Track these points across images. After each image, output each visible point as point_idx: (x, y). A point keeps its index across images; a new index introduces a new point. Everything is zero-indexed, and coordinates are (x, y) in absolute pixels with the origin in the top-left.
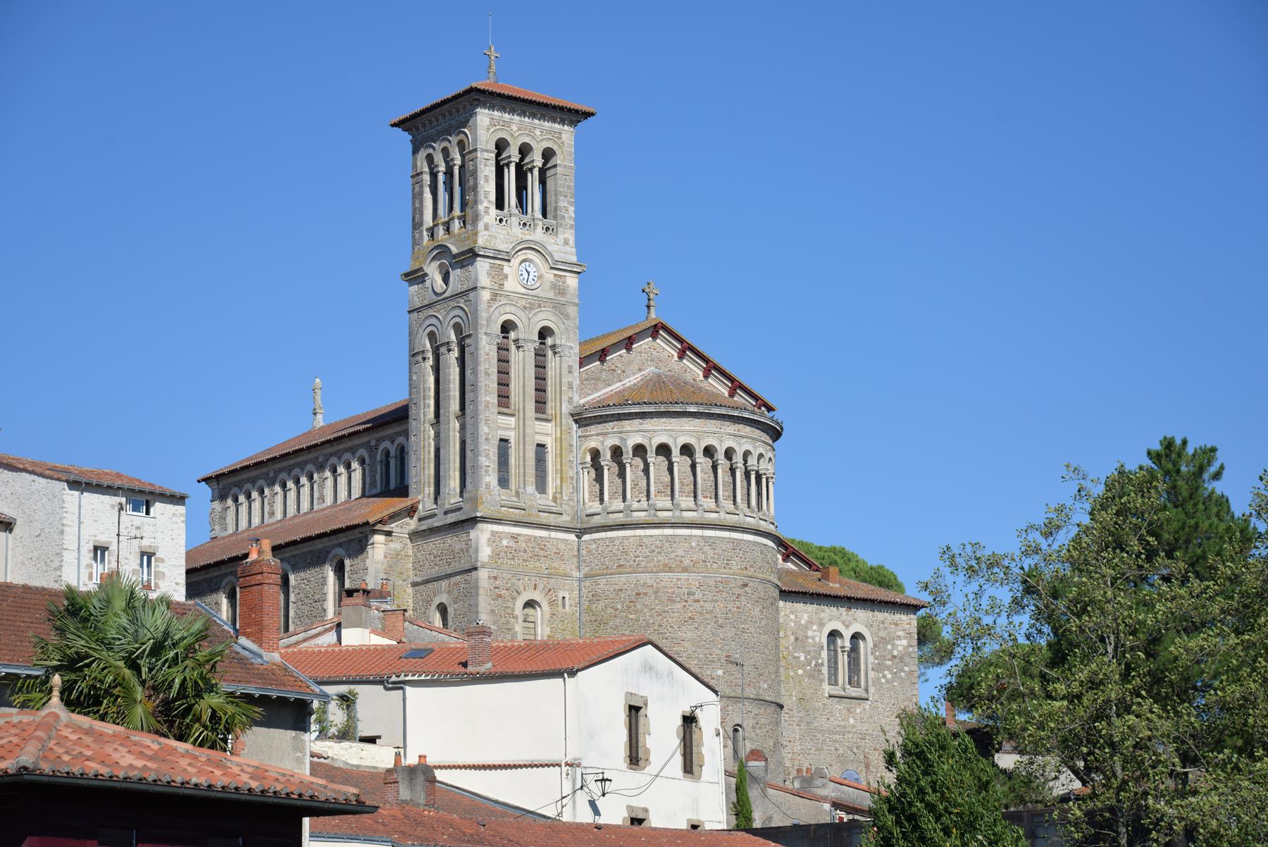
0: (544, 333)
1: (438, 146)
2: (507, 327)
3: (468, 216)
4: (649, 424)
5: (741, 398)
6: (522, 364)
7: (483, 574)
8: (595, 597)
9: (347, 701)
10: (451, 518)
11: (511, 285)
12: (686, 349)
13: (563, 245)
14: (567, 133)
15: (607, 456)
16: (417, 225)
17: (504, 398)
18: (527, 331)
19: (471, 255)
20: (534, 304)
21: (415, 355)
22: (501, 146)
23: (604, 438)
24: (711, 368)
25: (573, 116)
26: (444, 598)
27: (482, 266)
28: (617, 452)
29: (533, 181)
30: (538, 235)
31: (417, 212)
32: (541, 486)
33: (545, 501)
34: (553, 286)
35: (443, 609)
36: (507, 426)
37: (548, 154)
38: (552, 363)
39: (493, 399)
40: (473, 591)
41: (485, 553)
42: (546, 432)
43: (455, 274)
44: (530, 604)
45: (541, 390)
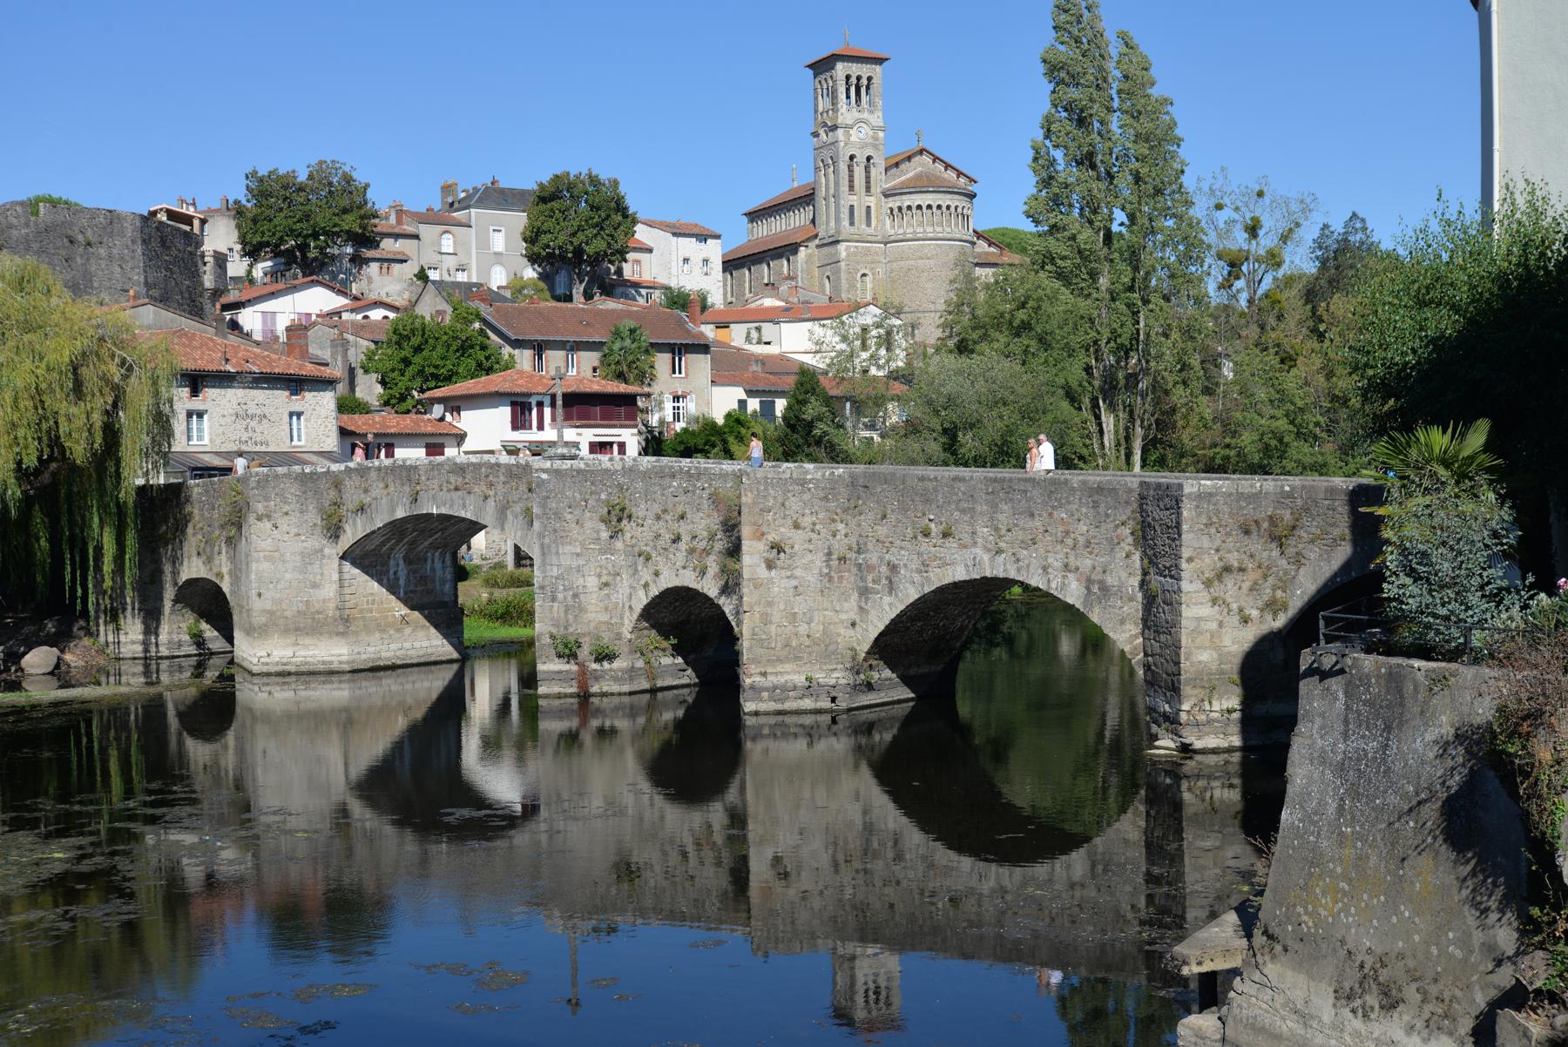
0: (869, 159)
1: (823, 77)
2: (852, 158)
3: (836, 110)
4: (913, 196)
5: (962, 180)
7: (843, 264)
8: (892, 271)
9: (758, 329)
10: (831, 240)
11: (853, 139)
12: (936, 159)
13: (877, 119)
14: (878, 68)
15: (896, 210)
16: (816, 111)
17: (851, 187)
18: (861, 159)
19: (834, 128)
20: (863, 146)
21: (817, 169)
22: (848, 77)
23: (894, 203)
24: (947, 166)
25: (880, 61)
26: (828, 273)
27: (840, 132)
28: (900, 209)
29: (863, 90)
30: (866, 115)
31: (816, 105)
32: (869, 224)
33: (870, 231)
34: (873, 137)
35: (828, 277)
36: (853, 200)
37: (869, 79)
38: (873, 171)
39: (846, 188)
40: (838, 271)
41: (843, 255)
42: (871, 201)
43: (830, 134)
44: (864, 275)
45: (868, 182)
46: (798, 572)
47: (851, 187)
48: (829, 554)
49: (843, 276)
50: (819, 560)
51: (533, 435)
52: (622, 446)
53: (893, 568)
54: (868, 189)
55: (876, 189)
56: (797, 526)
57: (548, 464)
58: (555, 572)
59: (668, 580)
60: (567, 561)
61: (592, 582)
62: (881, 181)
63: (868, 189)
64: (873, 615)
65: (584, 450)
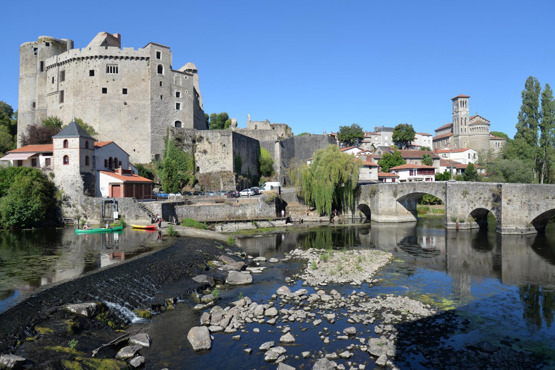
3: (458, 108)
5: (487, 122)
6: (463, 121)
12: (481, 117)
13: (467, 110)
14: (468, 99)
17: (462, 124)
18: (464, 118)
19: (458, 112)
20: (465, 115)
21: (453, 121)
23: (471, 127)
24: (483, 119)
25: (468, 97)
27: (459, 113)
30: (465, 109)
32: (465, 132)
33: (466, 133)
36: (462, 127)
38: (466, 121)
41: (460, 138)
42: (466, 127)
46: (514, 206)
47: (462, 124)
48: (522, 202)
49: (460, 143)
50: (519, 203)
51: (413, 177)
52: (432, 179)
53: (538, 205)
54: (465, 124)
55: (467, 124)
56: (514, 196)
57: (450, 183)
58: (452, 204)
59: (478, 206)
60: (454, 202)
61: (459, 207)
62: (468, 122)
63: (465, 124)
64: (532, 215)
65: (424, 180)
